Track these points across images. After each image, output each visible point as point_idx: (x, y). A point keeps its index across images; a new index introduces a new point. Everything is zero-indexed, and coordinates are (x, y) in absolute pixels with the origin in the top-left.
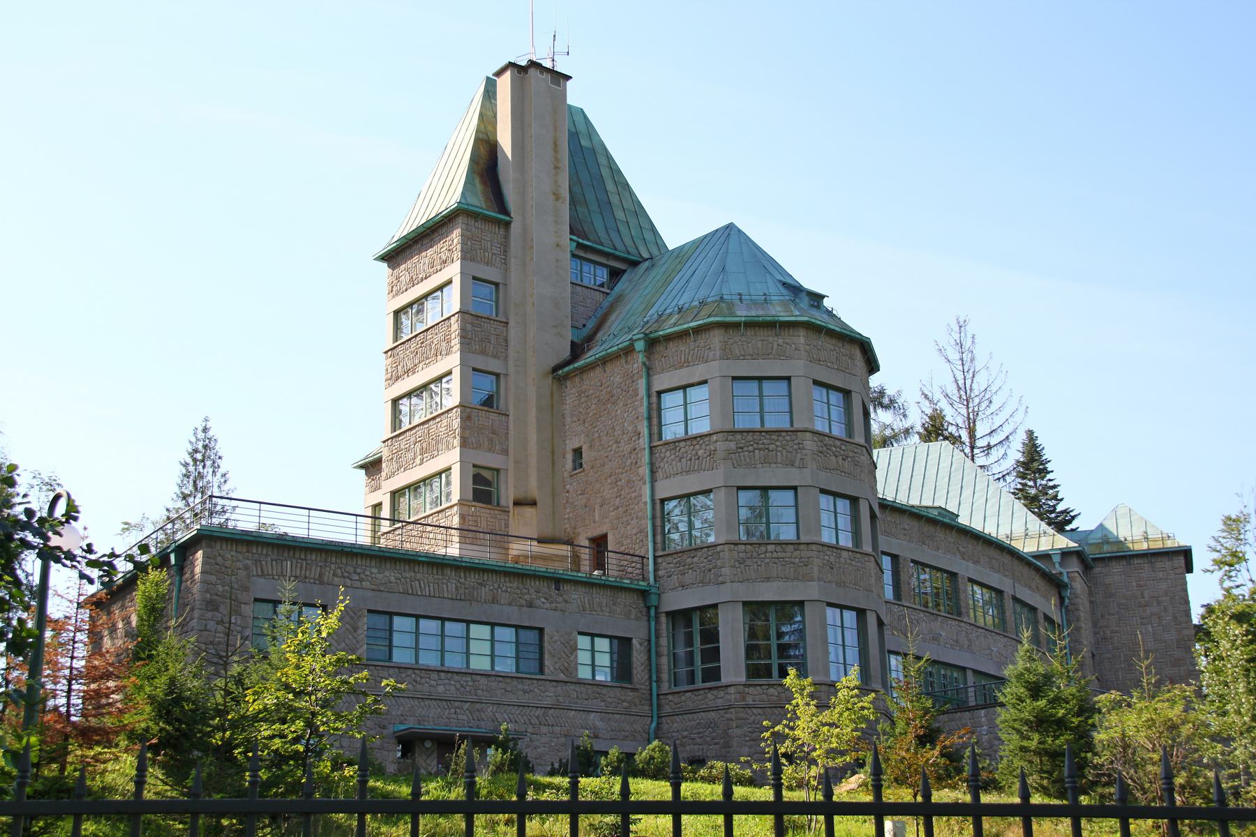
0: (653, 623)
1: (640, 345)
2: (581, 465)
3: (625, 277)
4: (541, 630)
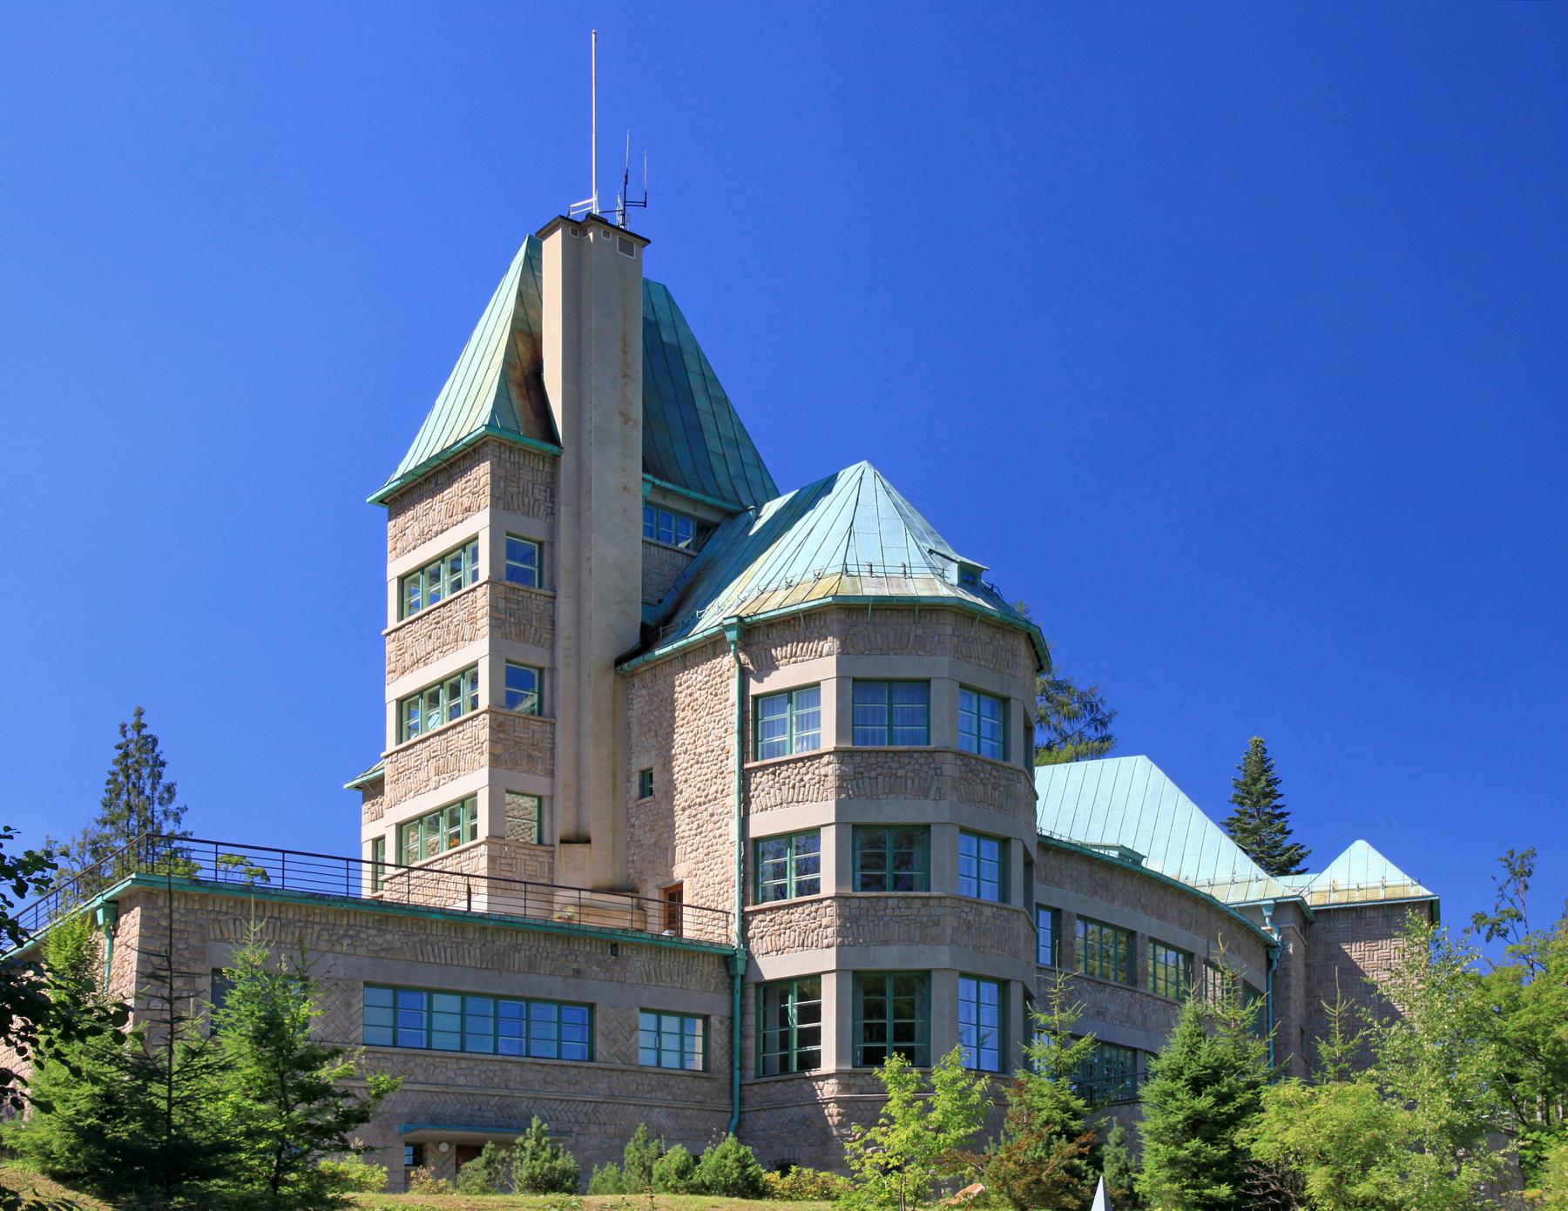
0: (738, 997)
1: (731, 635)
2: (651, 792)
3: (718, 533)
4: (592, 1006)
